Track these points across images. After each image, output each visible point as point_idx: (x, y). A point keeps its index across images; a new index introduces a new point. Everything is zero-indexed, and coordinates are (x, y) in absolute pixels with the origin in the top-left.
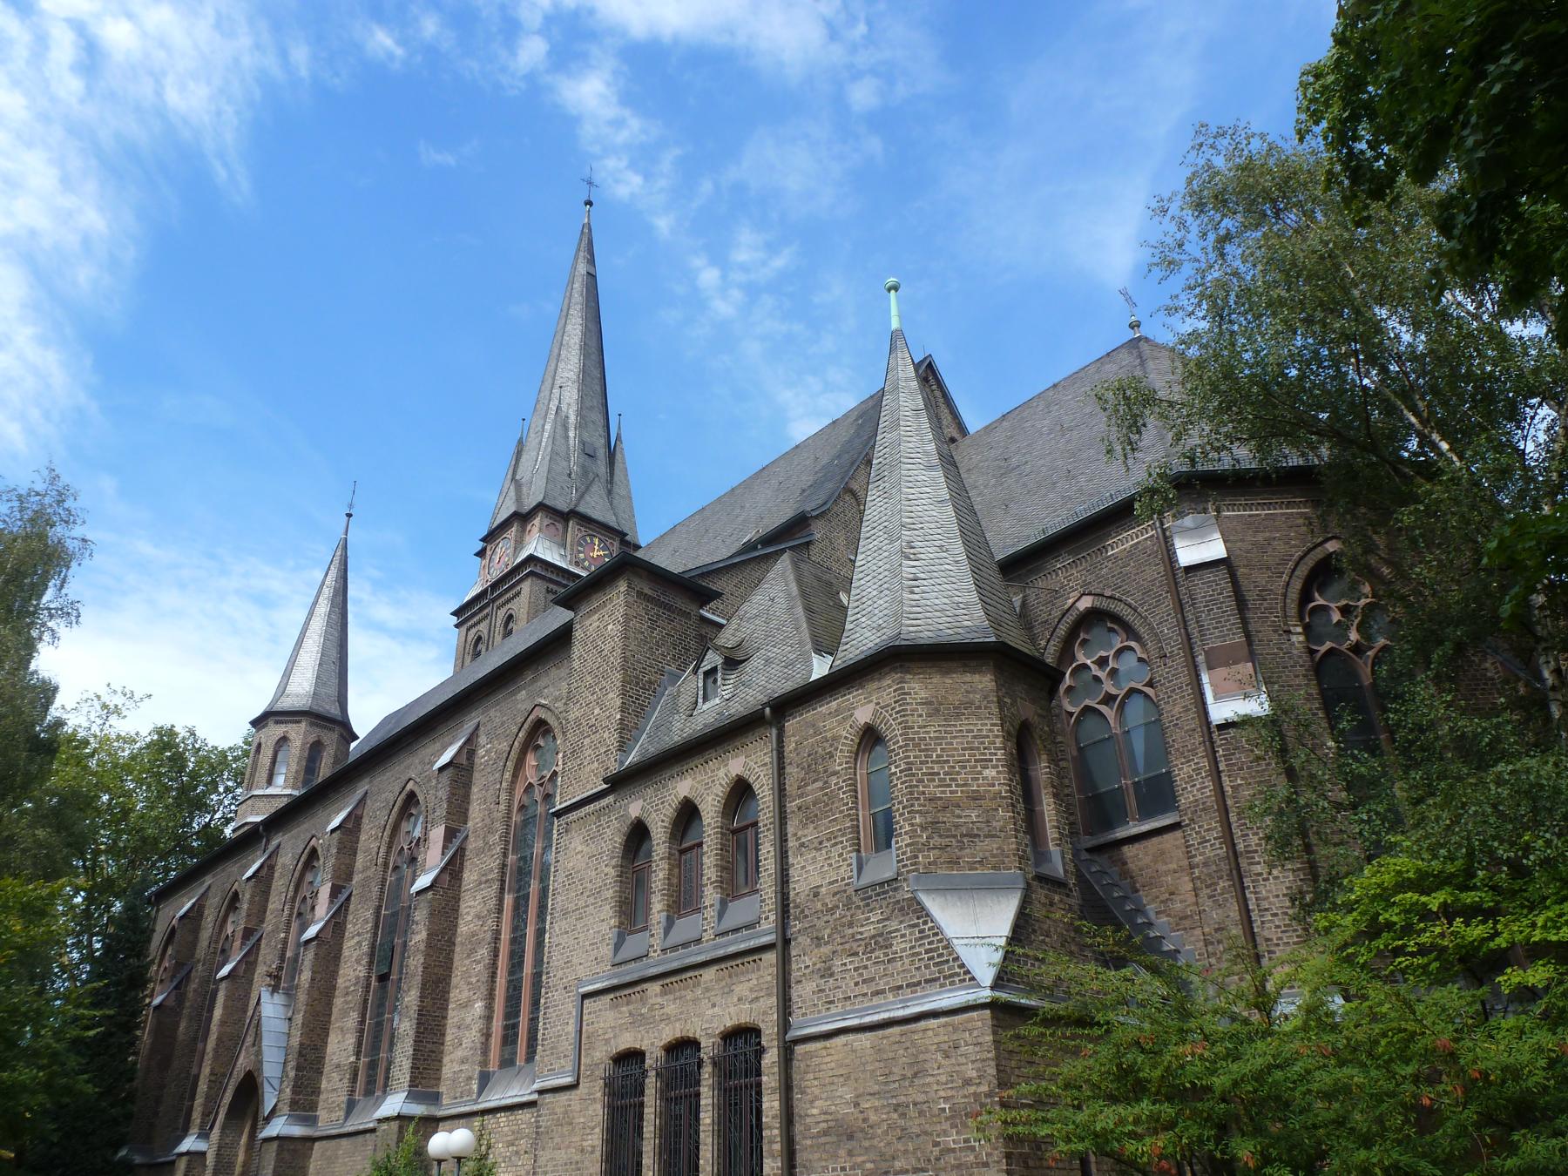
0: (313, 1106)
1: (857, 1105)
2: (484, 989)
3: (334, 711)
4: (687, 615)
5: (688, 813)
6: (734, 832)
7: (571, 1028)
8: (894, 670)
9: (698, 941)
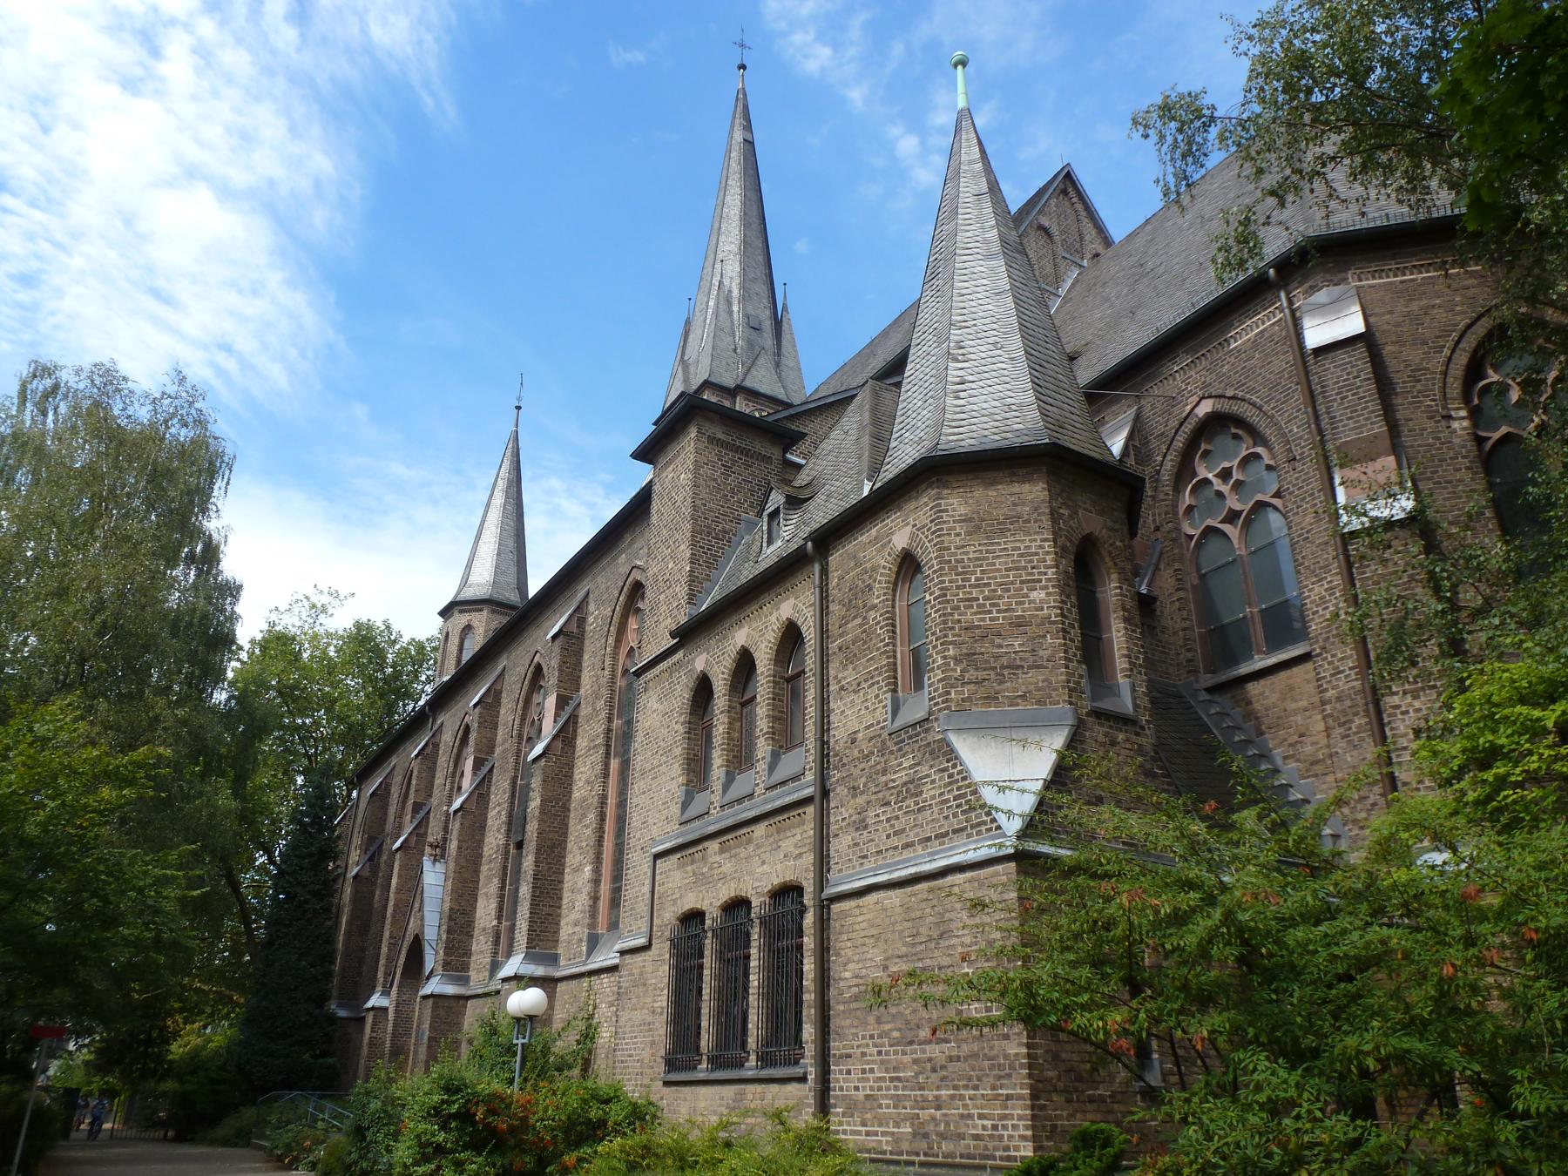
0: (465, 967)
1: (886, 968)
2: (591, 856)
4: (767, 460)
5: (745, 662)
6: (789, 680)
7: (646, 889)
8: (930, 486)
9: (751, 796)
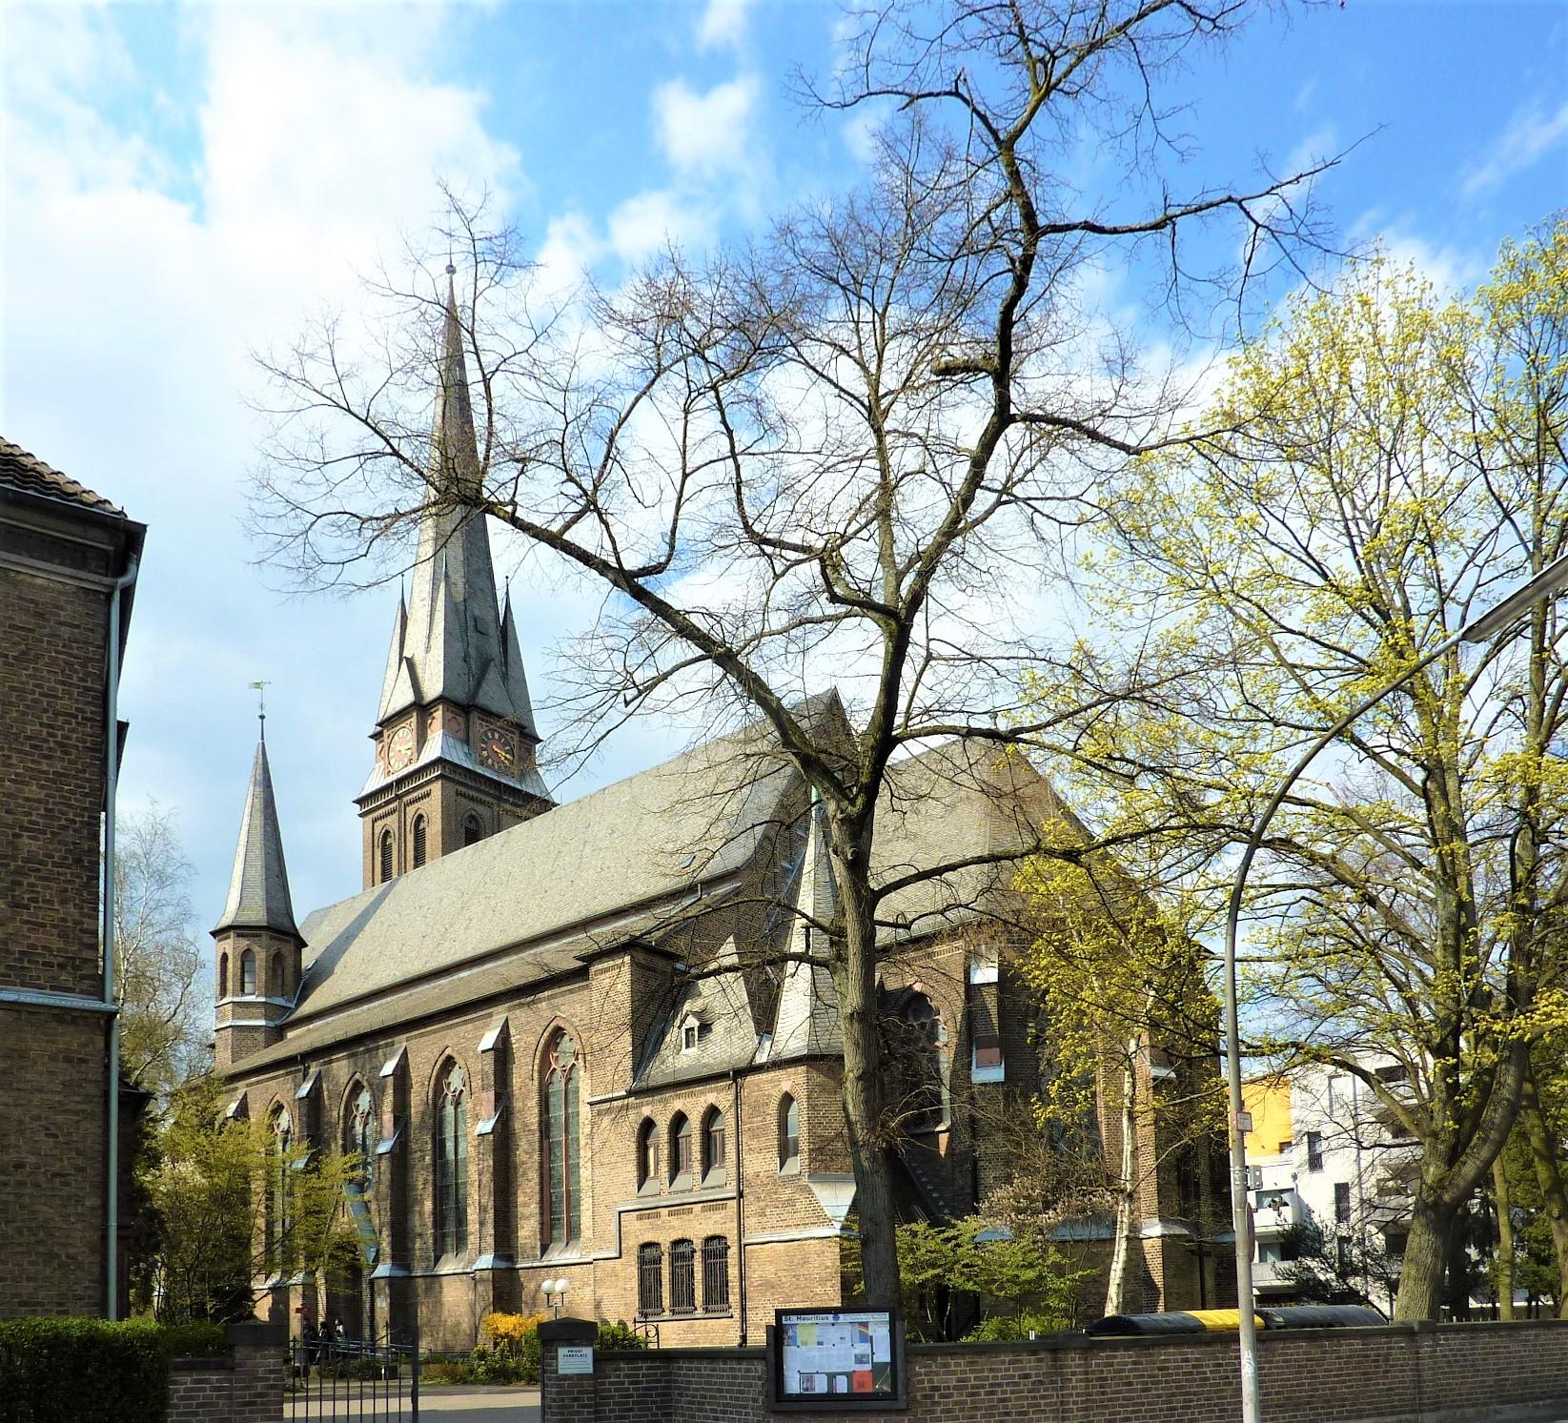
3: (286, 923)
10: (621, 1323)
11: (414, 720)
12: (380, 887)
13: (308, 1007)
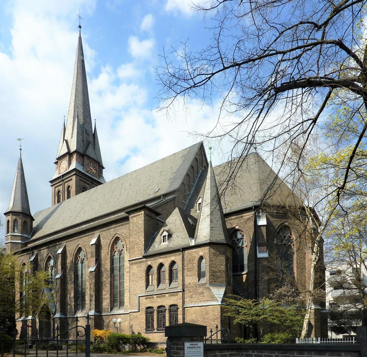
9: (165, 289)
10: (139, 333)
11: (67, 157)
12: (57, 205)
13: (34, 237)
